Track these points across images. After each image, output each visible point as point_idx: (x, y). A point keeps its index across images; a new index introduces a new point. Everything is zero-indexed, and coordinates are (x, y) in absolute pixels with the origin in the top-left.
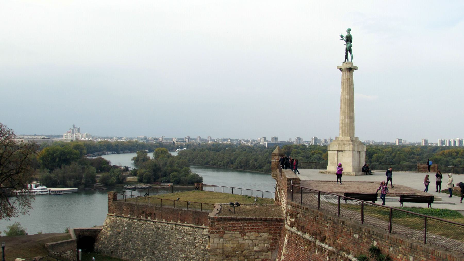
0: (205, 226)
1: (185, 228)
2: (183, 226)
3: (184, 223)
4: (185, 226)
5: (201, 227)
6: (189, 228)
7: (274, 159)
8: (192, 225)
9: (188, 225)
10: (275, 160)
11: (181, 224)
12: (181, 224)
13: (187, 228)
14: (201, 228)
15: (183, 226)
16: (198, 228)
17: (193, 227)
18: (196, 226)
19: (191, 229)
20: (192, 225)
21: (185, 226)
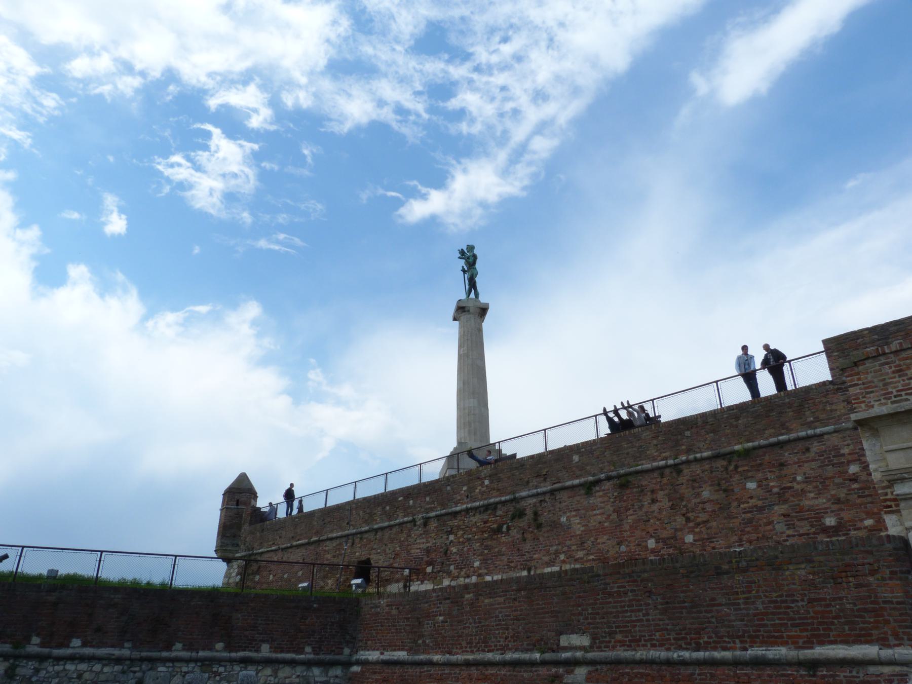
0: (187, 650)
1: (70, 667)
2: (58, 659)
3: (68, 646)
4: (72, 658)
5: (165, 654)
6: (97, 667)
7: (235, 503)
8: (116, 652)
9: (88, 651)
10: (237, 505)
11: (46, 650)
12: (46, 650)
13: (83, 666)
14: (164, 661)
15: (58, 659)
16: (150, 660)
17: (118, 660)
18: (136, 654)
19: (106, 670)
20: (116, 652)
21: (72, 658)
